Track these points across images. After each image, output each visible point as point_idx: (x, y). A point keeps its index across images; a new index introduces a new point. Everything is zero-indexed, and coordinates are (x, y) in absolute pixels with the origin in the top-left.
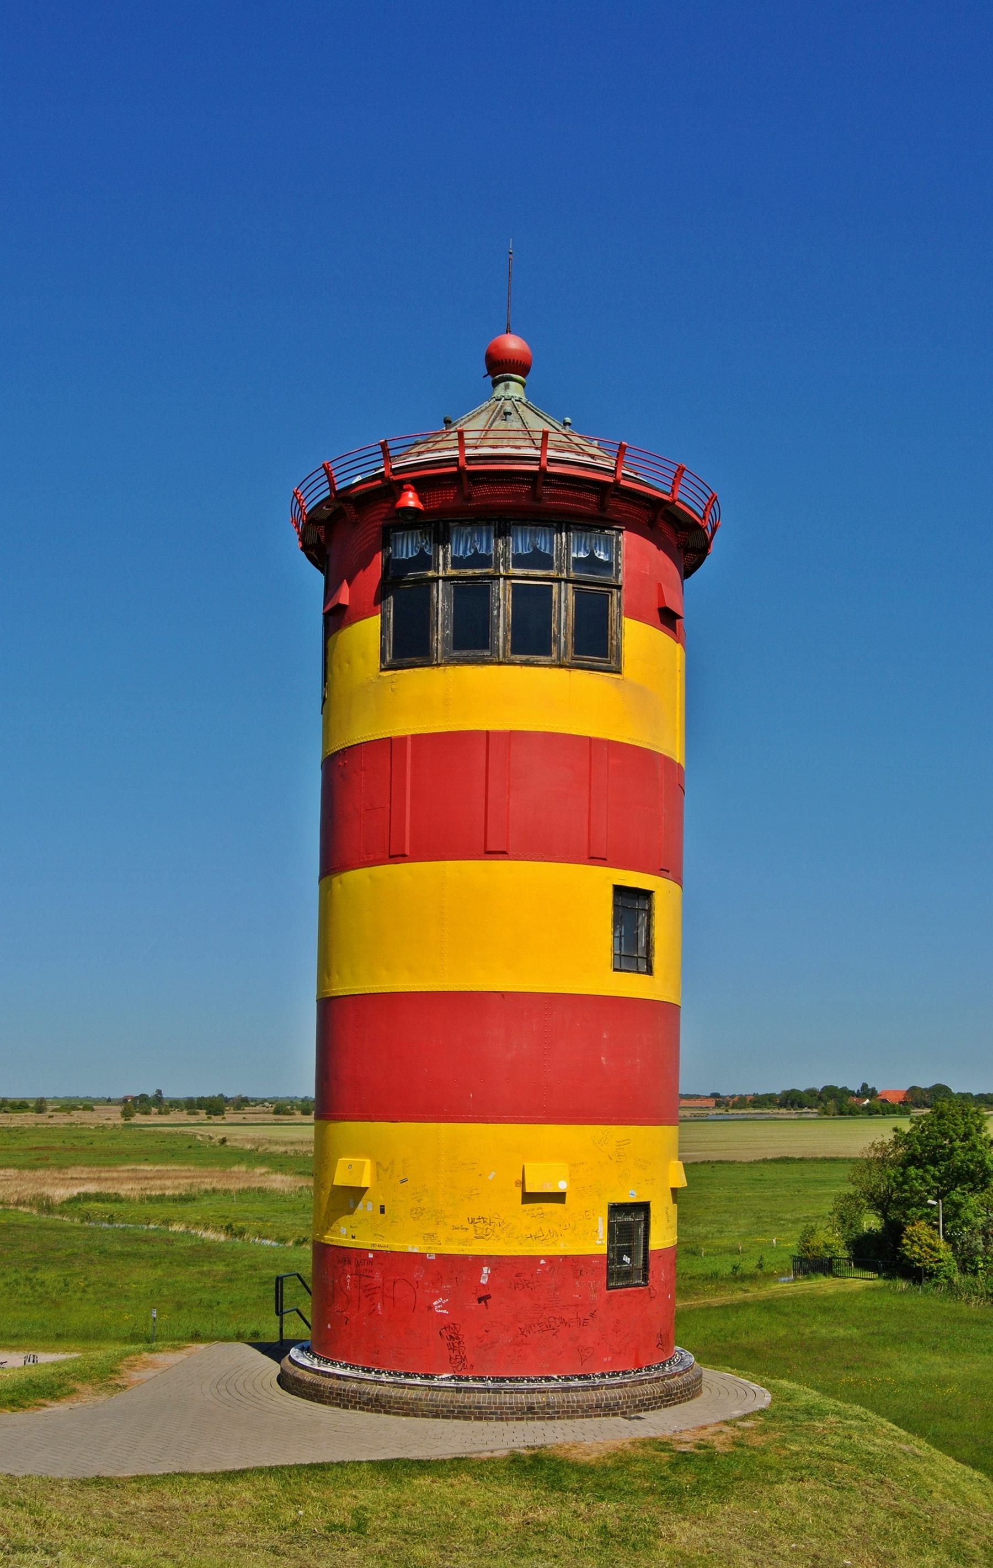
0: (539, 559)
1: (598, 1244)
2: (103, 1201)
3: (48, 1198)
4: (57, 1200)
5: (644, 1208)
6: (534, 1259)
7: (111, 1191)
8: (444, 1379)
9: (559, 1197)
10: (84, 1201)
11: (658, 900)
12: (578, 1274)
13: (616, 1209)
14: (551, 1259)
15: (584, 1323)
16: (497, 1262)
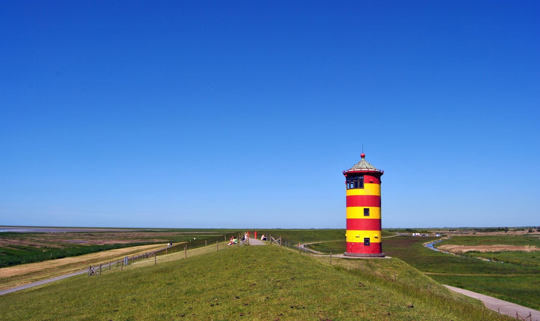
0: (356, 179)
1: (363, 241)
2: (475, 253)
3: (462, 251)
4: (464, 252)
5: (369, 238)
6: (357, 243)
7: (478, 250)
8: (350, 253)
9: (359, 237)
10: (470, 252)
11: (370, 209)
12: (361, 244)
13: (365, 238)
14: (358, 243)
15: (361, 249)
16: (354, 243)
